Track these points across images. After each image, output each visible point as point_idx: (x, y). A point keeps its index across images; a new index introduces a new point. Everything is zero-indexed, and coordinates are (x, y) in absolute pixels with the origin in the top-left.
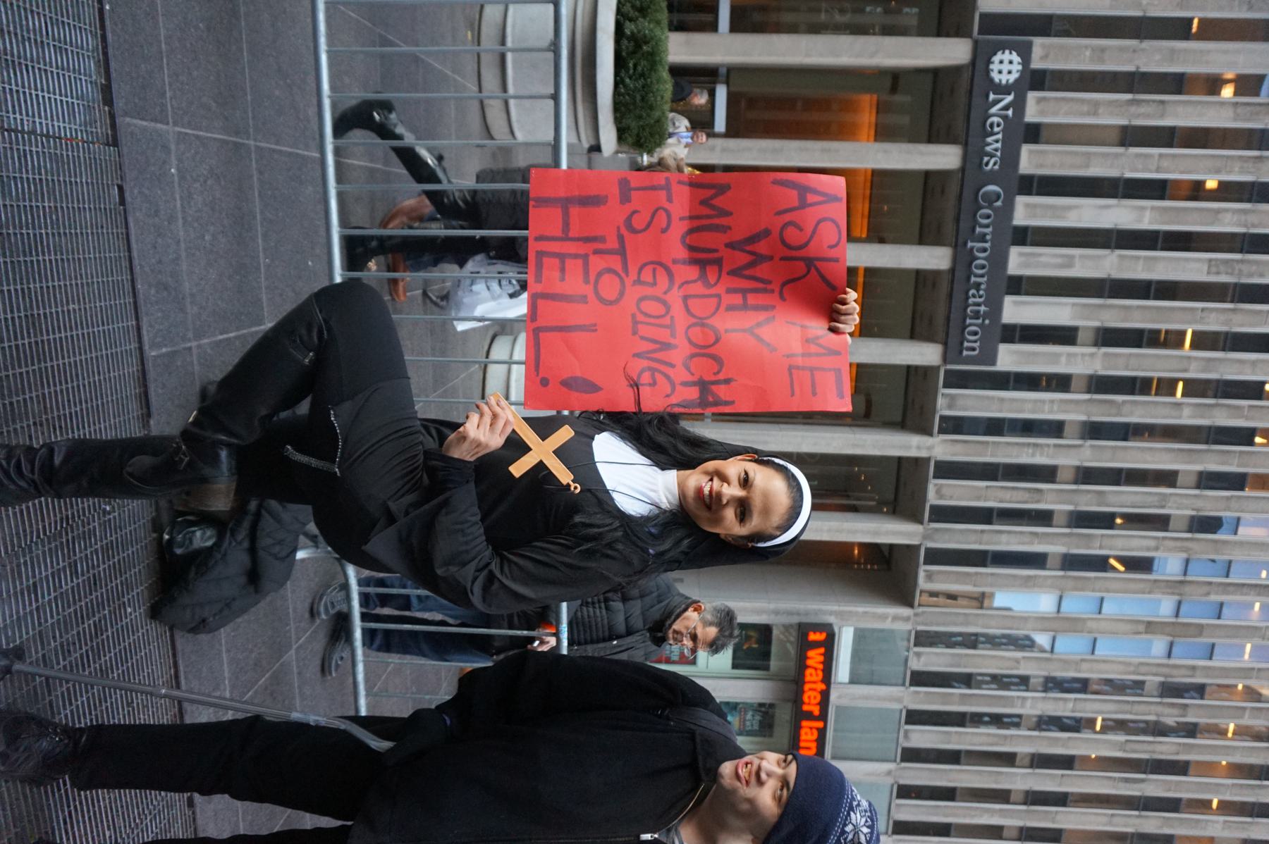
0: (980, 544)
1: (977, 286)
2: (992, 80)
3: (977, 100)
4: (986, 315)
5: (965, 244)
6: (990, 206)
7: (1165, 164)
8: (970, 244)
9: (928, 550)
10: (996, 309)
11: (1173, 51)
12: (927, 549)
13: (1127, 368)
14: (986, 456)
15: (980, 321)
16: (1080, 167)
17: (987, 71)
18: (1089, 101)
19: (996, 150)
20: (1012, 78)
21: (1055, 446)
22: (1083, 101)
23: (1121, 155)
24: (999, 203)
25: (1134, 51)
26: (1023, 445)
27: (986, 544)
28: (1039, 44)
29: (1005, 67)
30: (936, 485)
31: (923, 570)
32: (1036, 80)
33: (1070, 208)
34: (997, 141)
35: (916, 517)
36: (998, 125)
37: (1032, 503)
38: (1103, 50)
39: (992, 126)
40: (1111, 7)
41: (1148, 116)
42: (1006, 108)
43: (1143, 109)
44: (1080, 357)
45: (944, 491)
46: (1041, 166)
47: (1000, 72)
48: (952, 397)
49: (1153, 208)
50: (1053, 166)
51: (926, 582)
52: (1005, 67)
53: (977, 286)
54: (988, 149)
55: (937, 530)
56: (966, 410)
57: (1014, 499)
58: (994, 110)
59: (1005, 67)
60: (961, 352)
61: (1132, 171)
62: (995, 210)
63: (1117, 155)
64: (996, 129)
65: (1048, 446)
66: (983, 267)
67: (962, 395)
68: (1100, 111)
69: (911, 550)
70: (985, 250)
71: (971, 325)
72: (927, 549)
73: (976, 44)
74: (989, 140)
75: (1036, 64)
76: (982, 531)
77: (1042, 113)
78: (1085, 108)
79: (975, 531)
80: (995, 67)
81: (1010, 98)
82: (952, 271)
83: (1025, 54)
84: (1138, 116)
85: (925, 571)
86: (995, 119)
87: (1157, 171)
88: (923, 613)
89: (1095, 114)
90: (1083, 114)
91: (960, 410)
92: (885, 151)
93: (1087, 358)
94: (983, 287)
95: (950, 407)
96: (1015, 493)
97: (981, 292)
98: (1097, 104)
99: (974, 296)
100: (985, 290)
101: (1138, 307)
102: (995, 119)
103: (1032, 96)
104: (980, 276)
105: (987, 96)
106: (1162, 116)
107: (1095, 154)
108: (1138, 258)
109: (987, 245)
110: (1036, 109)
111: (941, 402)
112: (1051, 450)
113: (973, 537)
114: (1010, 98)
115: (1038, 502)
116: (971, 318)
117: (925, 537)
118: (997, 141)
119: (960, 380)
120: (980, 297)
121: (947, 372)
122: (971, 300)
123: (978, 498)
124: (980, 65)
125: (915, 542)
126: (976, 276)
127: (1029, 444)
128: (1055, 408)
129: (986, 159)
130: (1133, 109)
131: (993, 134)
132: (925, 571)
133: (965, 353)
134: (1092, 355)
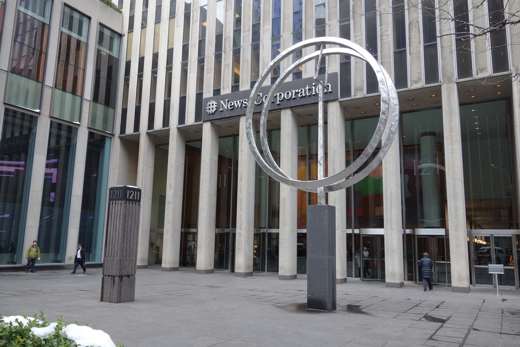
0: (452, 46)
1: (297, 93)
2: (215, 111)
3: (223, 115)
4: (310, 85)
5: (278, 104)
6: (262, 98)
7: (247, 29)
8: (278, 103)
9: (460, 76)
10: (310, 80)
11: (209, 43)
12: (459, 78)
13: (335, 7)
14: (390, 61)
15: (314, 87)
16: (248, 63)
17: (213, 114)
18: (224, 69)
19: (240, 102)
20: (215, 103)
21: (381, 25)
22: (224, 71)
23: (243, 48)
24: (261, 94)
25: (208, 58)
26: (381, 43)
27: (451, 42)
28: (206, 95)
29: (211, 107)
30: (411, 85)
31: (476, 75)
32: (217, 92)
33: (264, 62)
34: (237, 102)
35: (438, 91)
36: (231, 104)
37: (419, 25)
38: (208, 70)
39: (230, 107)
40: (195, 72)
41: (230, 43)
42: (225, 102)
43: (227, 46)
44: (331, 32)
45: (415, 78)
46: (247, 80)
47: (213, 109)
48: (356, 90)
49: (263, 26)
50: (248, 76)
51: (487, 71)
52: (212, 107)
53: (297, 93)
54: (240, 106)
55: (444, 76)
56: (363, 81)
57: (417, 36)
58: (226, 107)
59: (212, 107)
60: (330, 92)
61: (249, 41)
62: (263, 96)
63: (243, 50)
64: (233, 104)
65: (381, 29)
66: (288, 93)
67: (355, 85)
68: (228, 63)
69: (462, 89)
70: (281, 94)
71: (315, 91)
72: (459, 78)
73: (204, 122)
74: (236, 106)
75: (211, 95)
76: (442, 47)
77: (228, 87)
78: (227, 69)
79: (442, 52)
80: (211, 111)
81: (222, 102)
82: (291, 108)
83: (209, 99)
84: (230, 47)
85: (477, 74)
86: (229, 105)
87: (249, 31)
88: (513, 66)
89: (229, 65)
90: (229, 70)
91: (363, 84)
92: (242, 151)
93: (331, 28)
94: (297, 91)
95: (361, 90)
96: (413, 37)
97: (300, 91)
98: (225, 65)
99: (301, 94)
100: (298, 90)
101: (305, 14)
102: (229, 105)
103: (223, 93)
104: (292, 94)
105: (221, 111)
106: (230, 38)
107: (243, 59)
108: (284, 23)
109: (278, 94)
110: (226, 89)
111: (359, 96)
112: (383, 27)
113: (447, 51)
114: (222, 102)
115: (418, 22)
116: (312, 92)
117: (450, 81)
118: (237, 102)
119: (346, 90)
120: (302, 90)
121: (341, 97)
122: (303, 95)
123: (419, 57)
124: (211, 118)
125: (455, 87)
126: (292, 96)
127: (381, 40)
128: (359, 33)
129: (244, 105)
130: (227, 50)
131: (234, 106)
132: (477, 74)
133: (330, 90)
134: (329, 26)
